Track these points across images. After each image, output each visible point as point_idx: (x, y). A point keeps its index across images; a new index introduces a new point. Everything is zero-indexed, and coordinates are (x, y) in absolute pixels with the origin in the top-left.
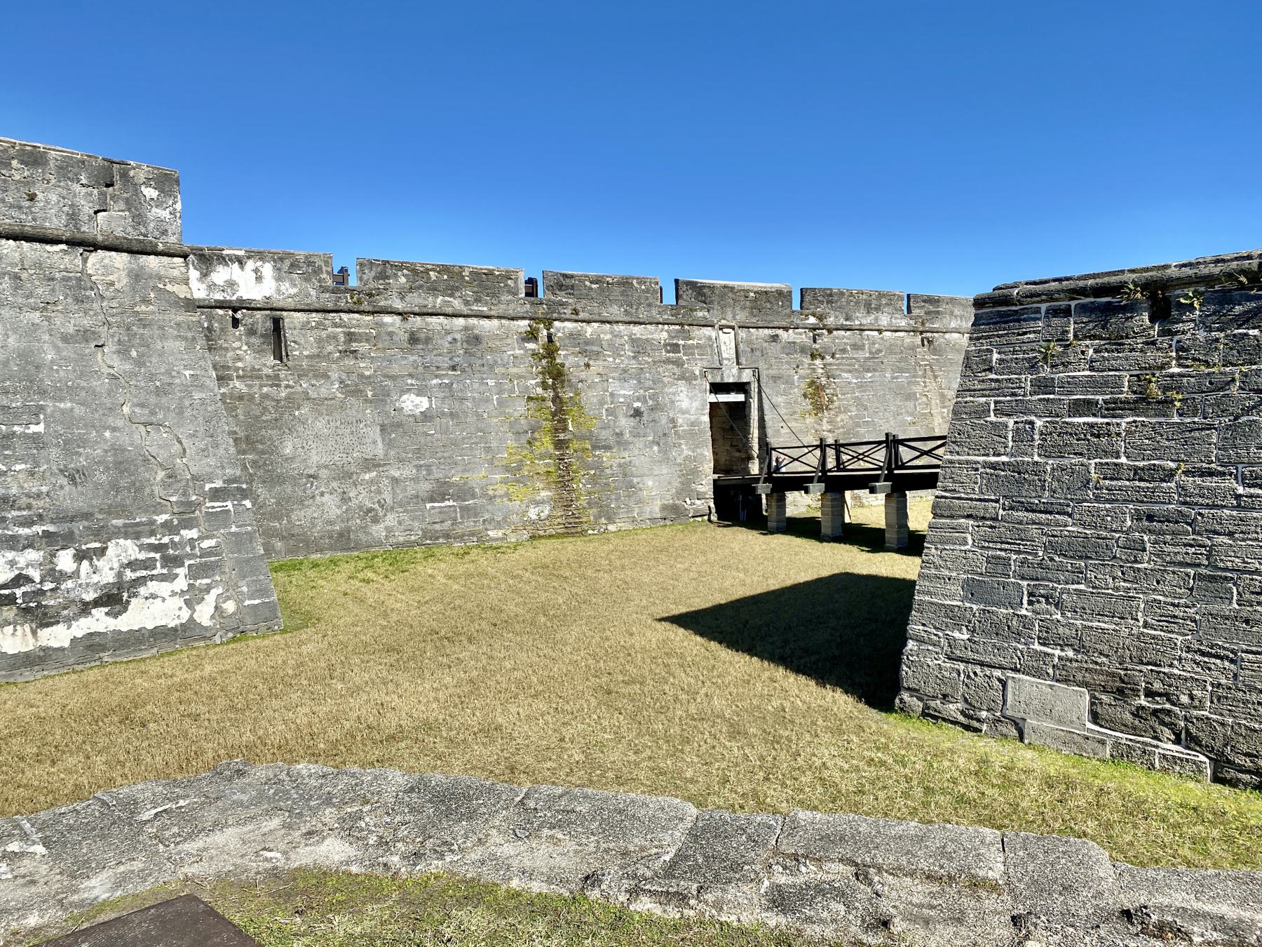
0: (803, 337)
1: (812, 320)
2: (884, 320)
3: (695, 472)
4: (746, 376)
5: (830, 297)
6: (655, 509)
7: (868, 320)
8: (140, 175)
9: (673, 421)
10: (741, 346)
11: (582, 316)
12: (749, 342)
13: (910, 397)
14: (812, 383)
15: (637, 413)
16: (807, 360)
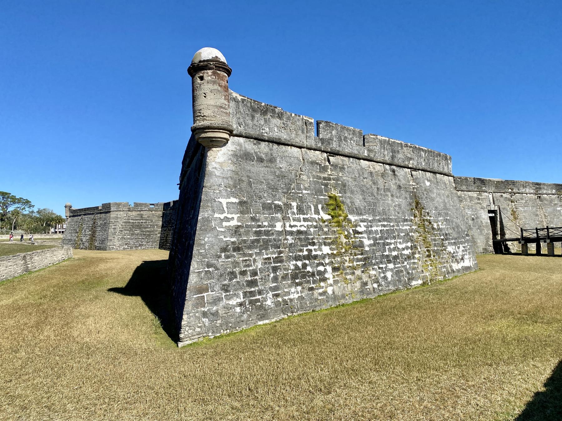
0: (508, 196)
1: (510, 190)
2: (527, 191)
3: (488, 238)
4: (496, 208)
5: (513, 183)
6: (481, 250)
7: (524, 190)
8: (448, 157)
9: (481, 222)
10: (495, 199)
11: (458, 189)
12: (496, 197)
13: (537, 215)
14: (512, 211)
15: (473, 219)
16: (510, 203)
